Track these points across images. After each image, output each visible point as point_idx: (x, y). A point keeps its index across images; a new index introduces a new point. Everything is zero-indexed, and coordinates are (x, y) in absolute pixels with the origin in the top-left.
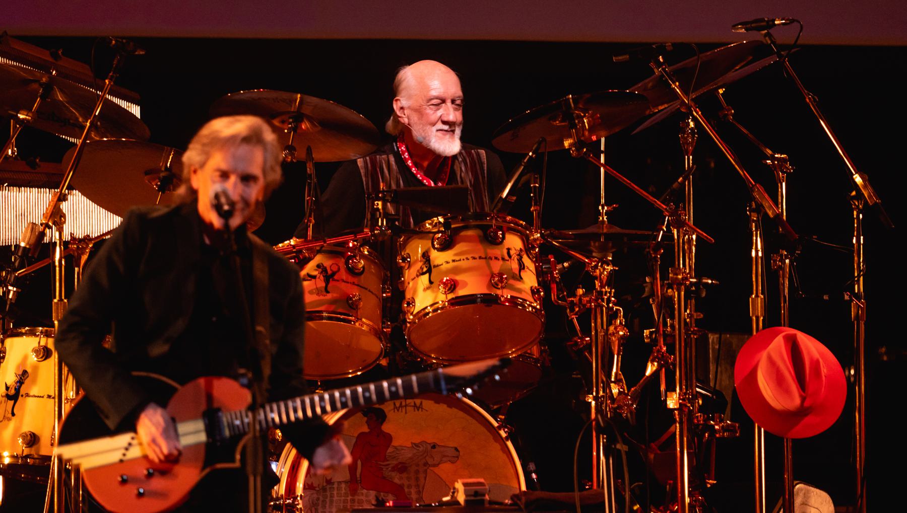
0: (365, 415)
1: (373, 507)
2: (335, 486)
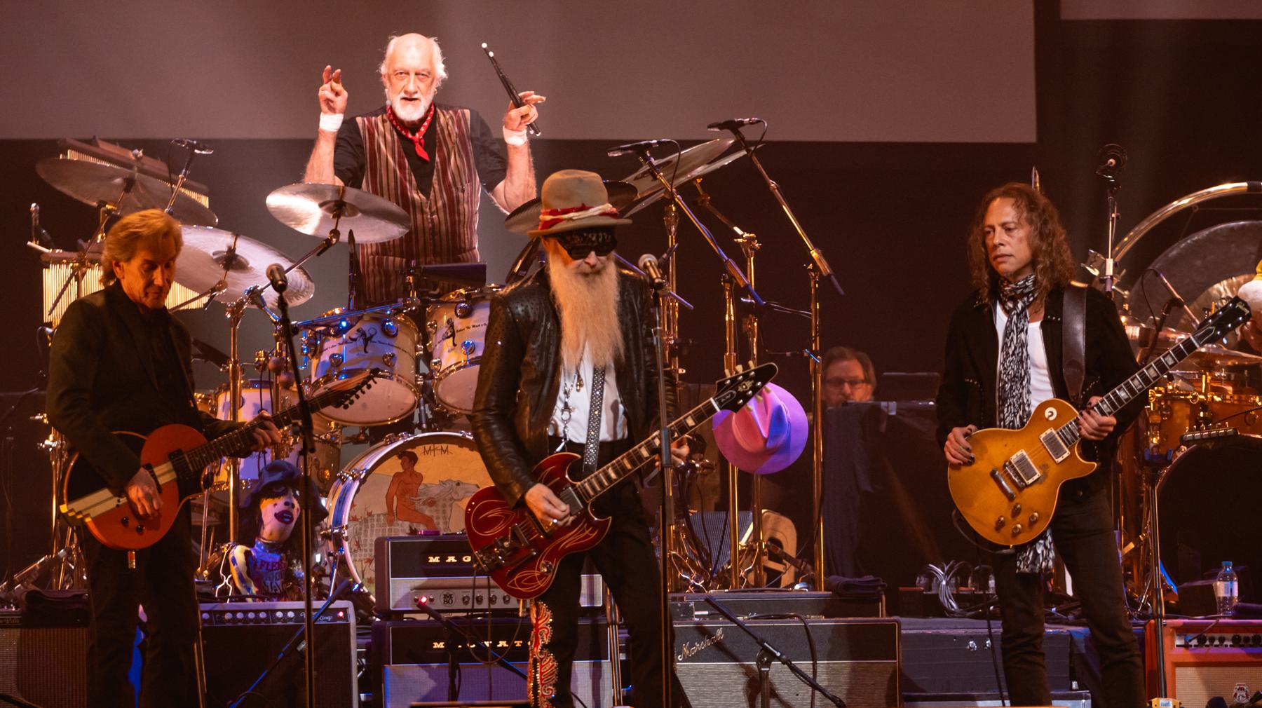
0: (400, 457)
1: (407, 535)
2: (375, 517)
